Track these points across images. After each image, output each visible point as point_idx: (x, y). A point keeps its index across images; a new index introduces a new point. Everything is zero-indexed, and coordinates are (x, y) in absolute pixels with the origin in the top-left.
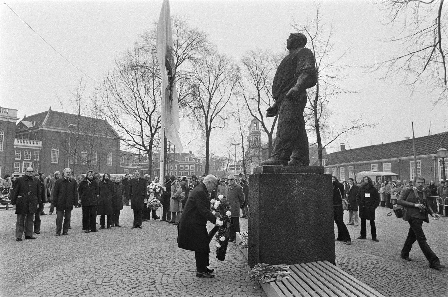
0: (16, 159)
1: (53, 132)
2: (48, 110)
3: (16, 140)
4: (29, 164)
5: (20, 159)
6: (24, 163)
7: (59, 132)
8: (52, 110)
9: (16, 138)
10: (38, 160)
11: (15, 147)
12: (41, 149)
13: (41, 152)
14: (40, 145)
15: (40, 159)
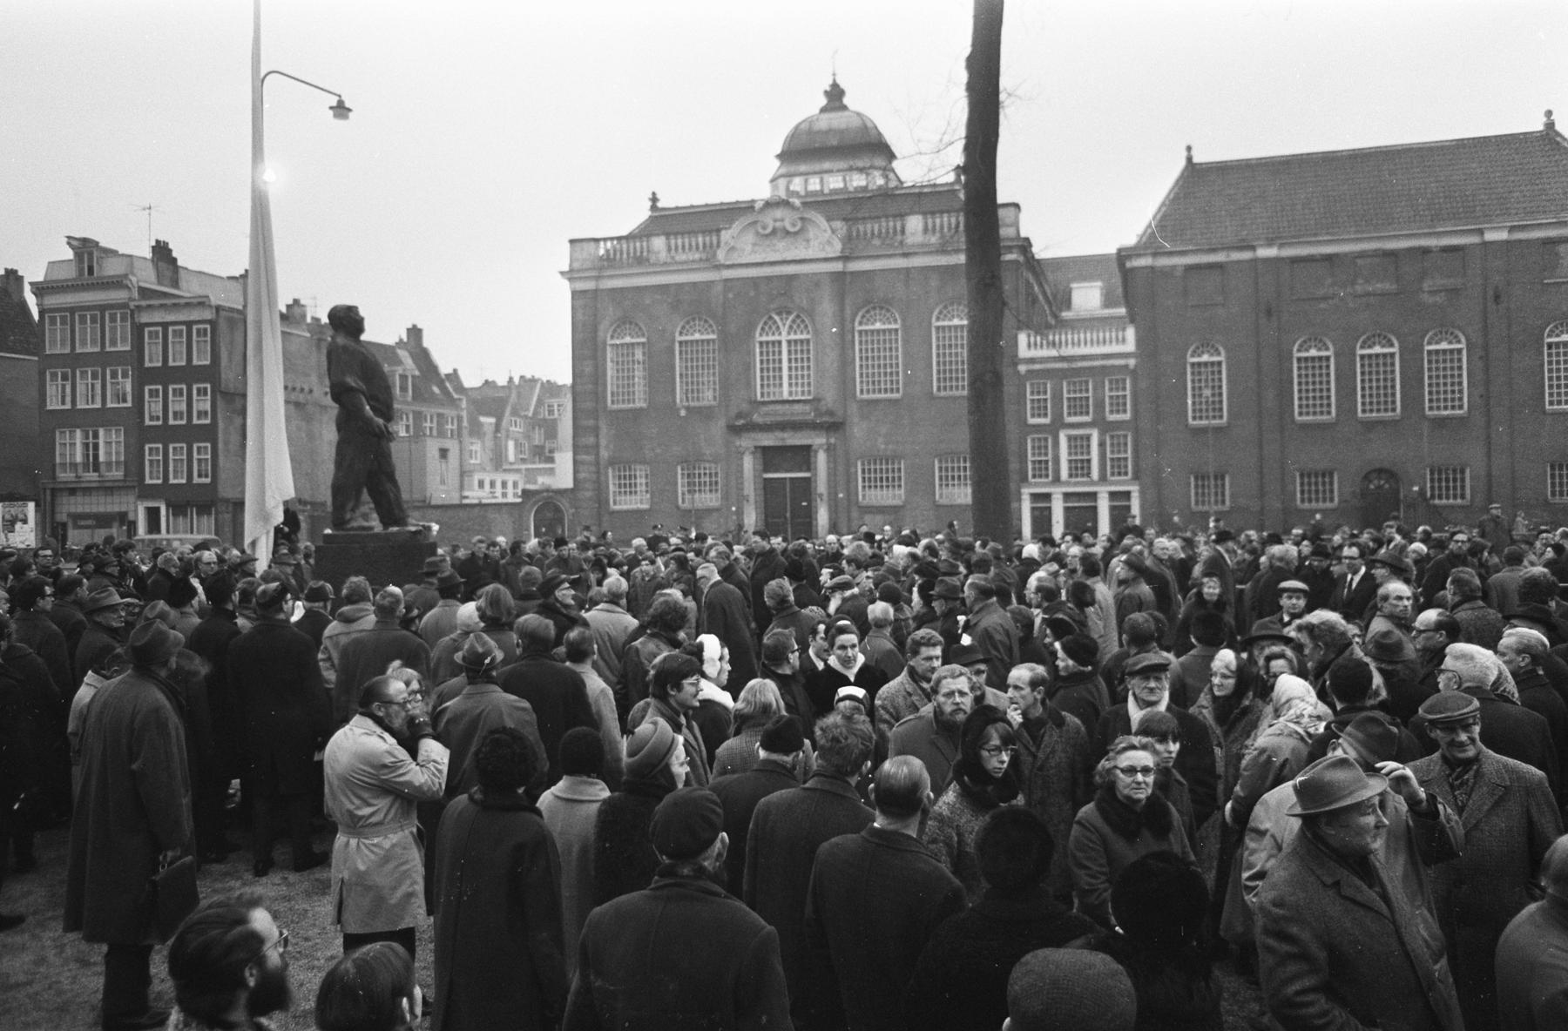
0: (1032, 421)
1: (1189, 268)
2: (1182, 163)
3: (1022, 338)
4: (1088, 438)
5: (1046, 421)
6: (1070, 438)
7: (1219, 266)
8: (1196, 160)
9: (1019, 328)
10: (1127, 416)
11: (1022, 368)
12: (1132, 362)
13: (1134, 373)
14: (1130, 346)
15: (1135, 411)
